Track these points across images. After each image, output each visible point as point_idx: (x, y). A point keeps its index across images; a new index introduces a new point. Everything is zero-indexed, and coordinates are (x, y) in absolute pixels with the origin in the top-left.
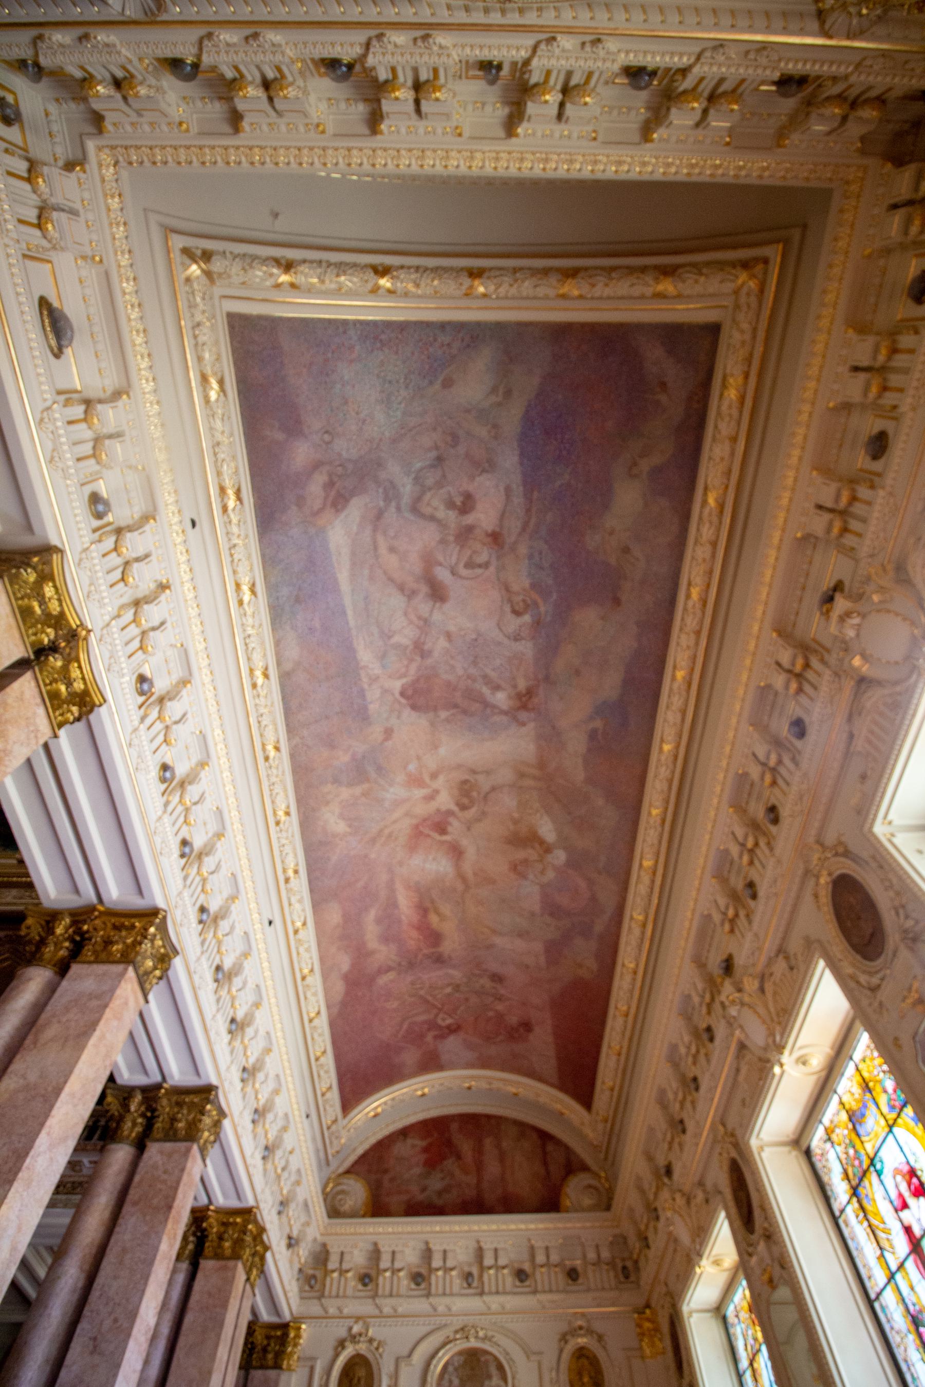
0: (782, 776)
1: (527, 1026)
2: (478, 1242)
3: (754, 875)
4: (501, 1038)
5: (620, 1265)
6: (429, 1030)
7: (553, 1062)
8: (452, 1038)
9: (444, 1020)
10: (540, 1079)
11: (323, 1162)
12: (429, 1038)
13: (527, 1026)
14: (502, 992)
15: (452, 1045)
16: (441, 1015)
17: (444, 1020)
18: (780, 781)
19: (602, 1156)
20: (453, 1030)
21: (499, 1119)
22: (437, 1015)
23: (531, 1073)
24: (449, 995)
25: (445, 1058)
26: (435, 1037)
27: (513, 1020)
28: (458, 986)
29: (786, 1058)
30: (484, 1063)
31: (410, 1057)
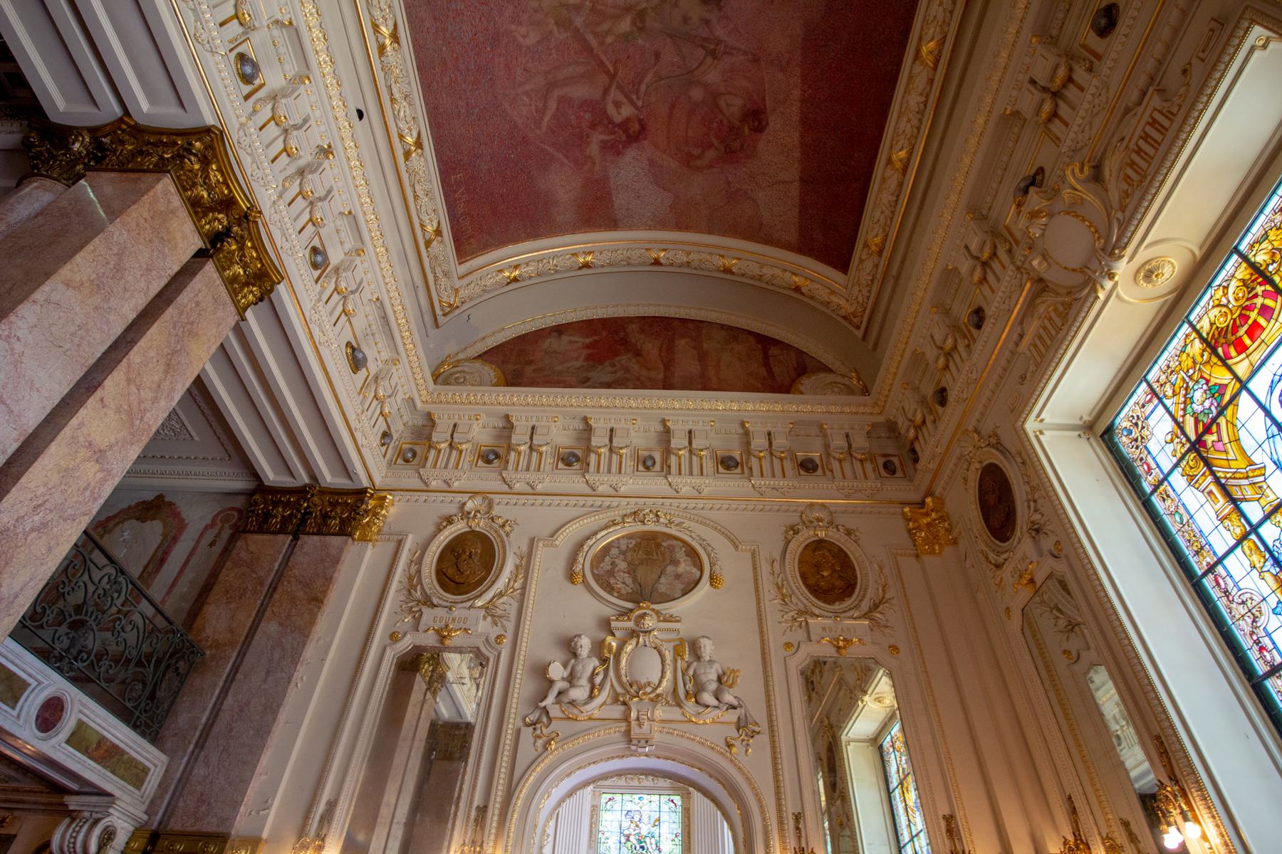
0: (994, 273)
1: (755, 117)
2: (664, 422)
3: (947, 381)
4: (711, 154)
5: (881, 461)
6: (593, 126)
7: (795, 191)
8: (631, 154)
9: (618, 105)
10: (768, 241)
11: (428, 318)
12: (594, 149)
13: (755, 117)
14: (720, 32)
15: (630, 172)
16: (614, 94)
17: (618, 105)
18: (990, 277)
19: (860, 334)
20: (633, 133)
21: (699, 324)
22: (606, 92)
23: (755, 232)
24: (626, 37)
25: (620, 200)
26: (605, 146)
27: (733, 106)
28: (641, 15)
29: (1123, 268)
30: (680, 217)
31: (562, 185)
